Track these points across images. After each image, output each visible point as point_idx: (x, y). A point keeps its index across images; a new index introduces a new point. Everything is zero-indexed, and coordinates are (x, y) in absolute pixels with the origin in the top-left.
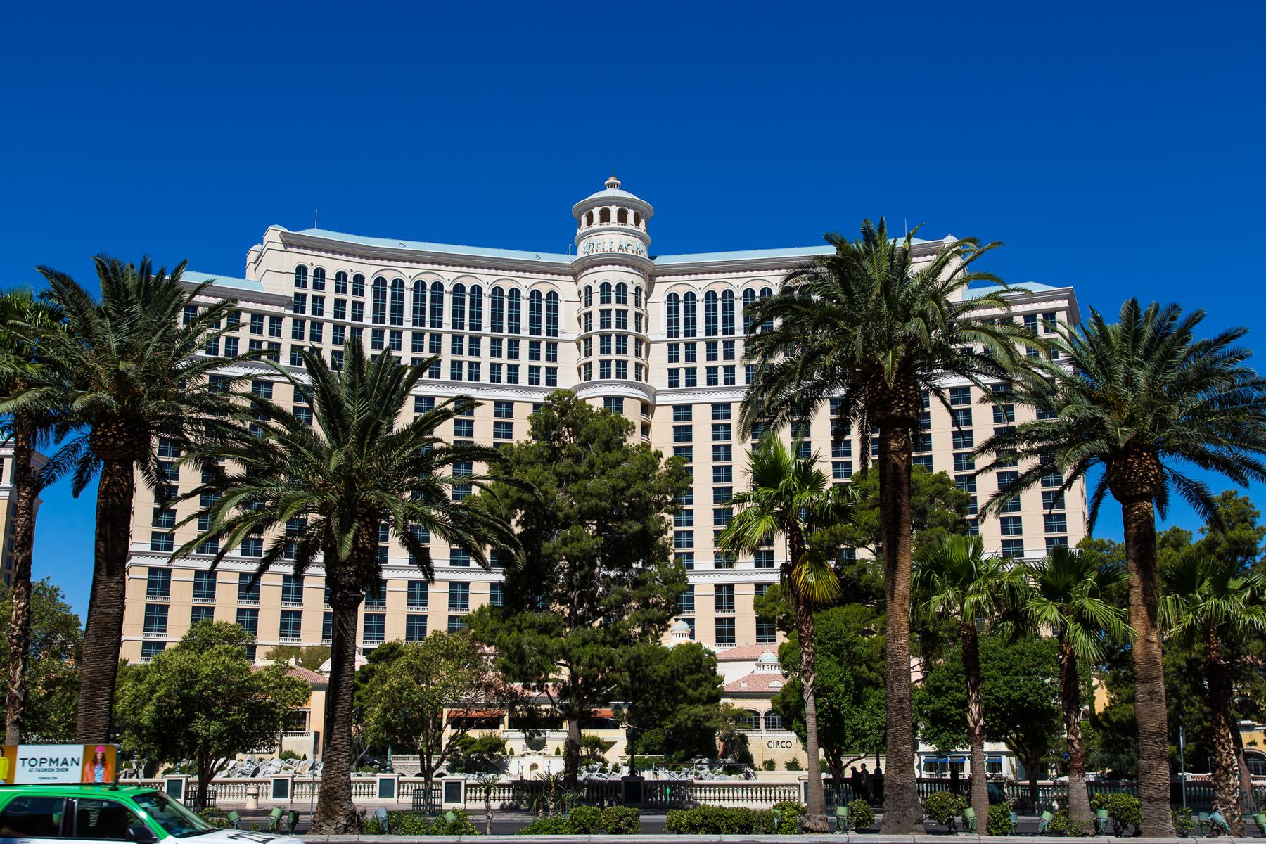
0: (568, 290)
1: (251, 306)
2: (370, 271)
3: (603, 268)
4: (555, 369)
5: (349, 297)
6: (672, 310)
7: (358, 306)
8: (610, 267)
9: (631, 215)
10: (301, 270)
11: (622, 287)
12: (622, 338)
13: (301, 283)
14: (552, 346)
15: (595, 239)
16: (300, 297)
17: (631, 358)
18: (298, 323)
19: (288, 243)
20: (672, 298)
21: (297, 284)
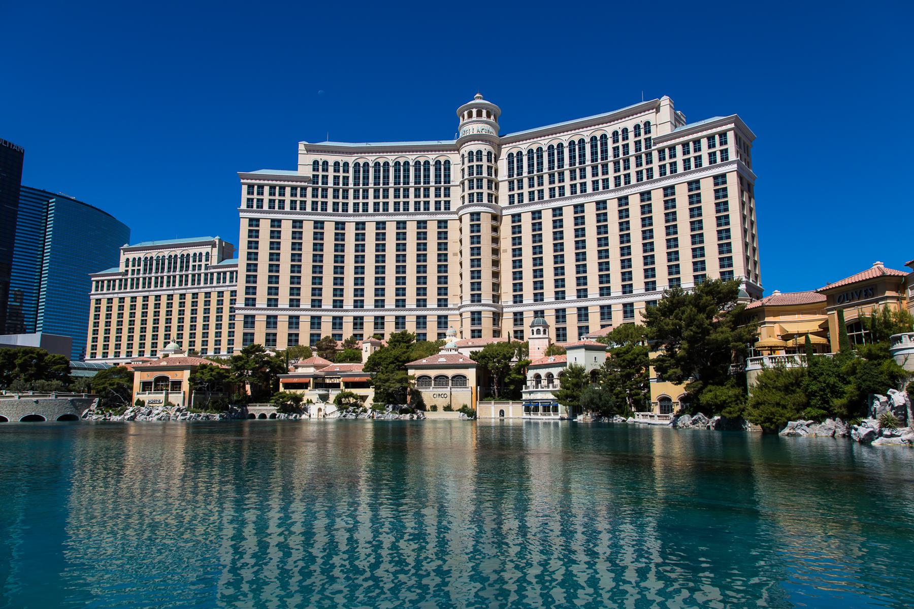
0: (455, 158)
2: (351, 160)
3: (469, 143)
4: (449, 202)
5: (341, 174)
6: (510, 163)
7: (346, 179)
8: (473, 142)
9: (484, 112)
10: (316, 163)
11: (479, 153)
12: (480, 180)
13: (315, 169)
14: (447, 189)
15: (465, 128)
16: (316, 177)
17: (485, 191)
18: (315, 190)
19: (309, 150)
20: (510, 156)
21: (314, 170)
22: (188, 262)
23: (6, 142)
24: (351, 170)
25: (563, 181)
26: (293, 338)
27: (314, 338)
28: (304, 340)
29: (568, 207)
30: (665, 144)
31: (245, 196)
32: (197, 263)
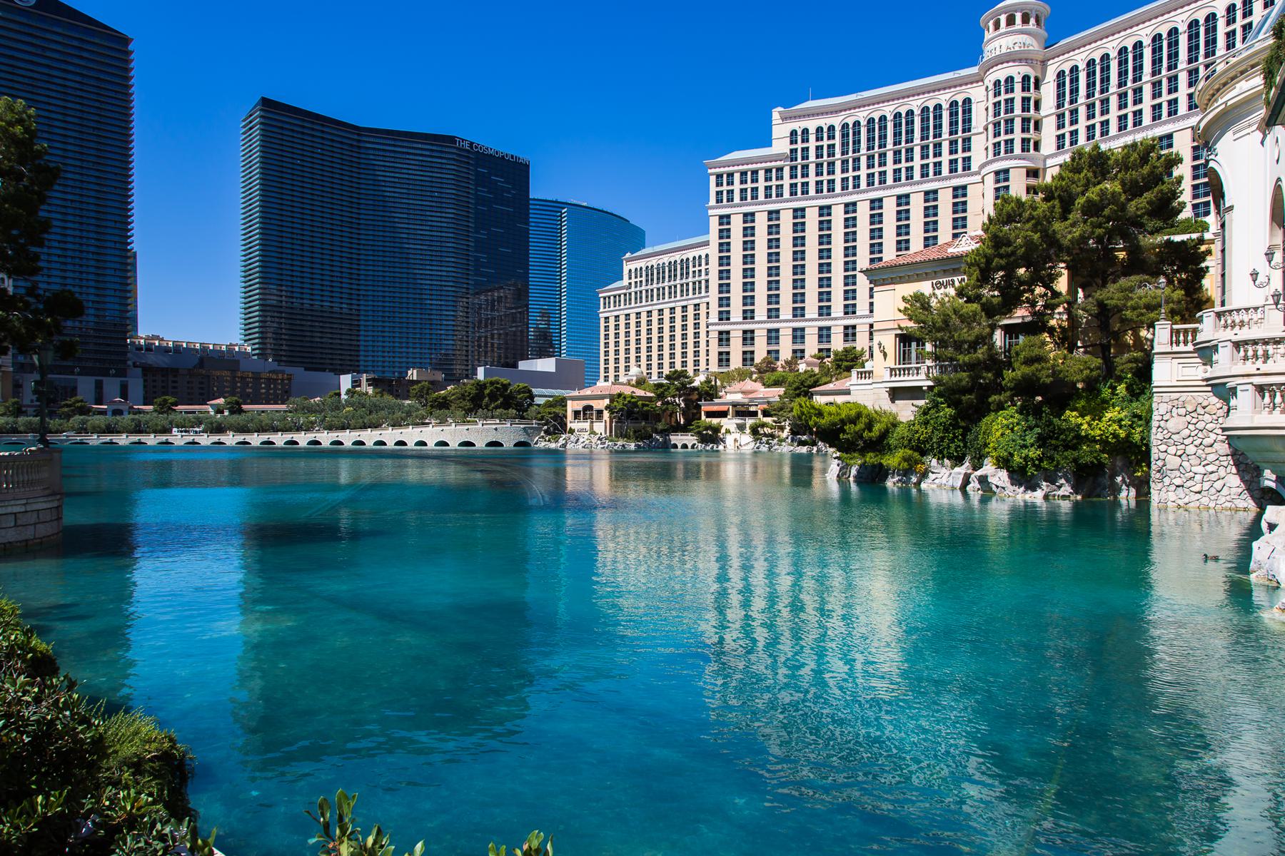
0: (980, 96)
1: (764, 165)
2: (837, 121)
3: (995, 68)
4: (969, 158)
6: (1061, 85)
8: (1000, 67)
10: (794, 133)
11: (1010, 80)
12: (1010, 122)
14: (967, 141)
15: (996, 44)
16: (793, 151)
18: (793, 168)
19: (785, 119)
20: (1061, 75)
22: (688, 268)
23: (512, 157)
24: (838, 134)
25: (912, 160)
26: (724, 357)
27: (748, 357)
28: (736, 362)
29: (837, 204)
30: (773, 164)
31: (713, 189)
32: (697, 269)
